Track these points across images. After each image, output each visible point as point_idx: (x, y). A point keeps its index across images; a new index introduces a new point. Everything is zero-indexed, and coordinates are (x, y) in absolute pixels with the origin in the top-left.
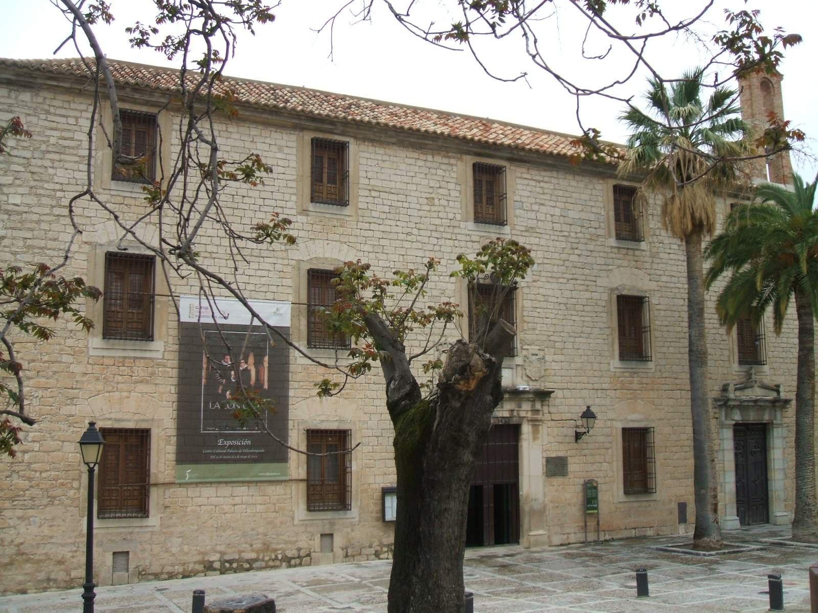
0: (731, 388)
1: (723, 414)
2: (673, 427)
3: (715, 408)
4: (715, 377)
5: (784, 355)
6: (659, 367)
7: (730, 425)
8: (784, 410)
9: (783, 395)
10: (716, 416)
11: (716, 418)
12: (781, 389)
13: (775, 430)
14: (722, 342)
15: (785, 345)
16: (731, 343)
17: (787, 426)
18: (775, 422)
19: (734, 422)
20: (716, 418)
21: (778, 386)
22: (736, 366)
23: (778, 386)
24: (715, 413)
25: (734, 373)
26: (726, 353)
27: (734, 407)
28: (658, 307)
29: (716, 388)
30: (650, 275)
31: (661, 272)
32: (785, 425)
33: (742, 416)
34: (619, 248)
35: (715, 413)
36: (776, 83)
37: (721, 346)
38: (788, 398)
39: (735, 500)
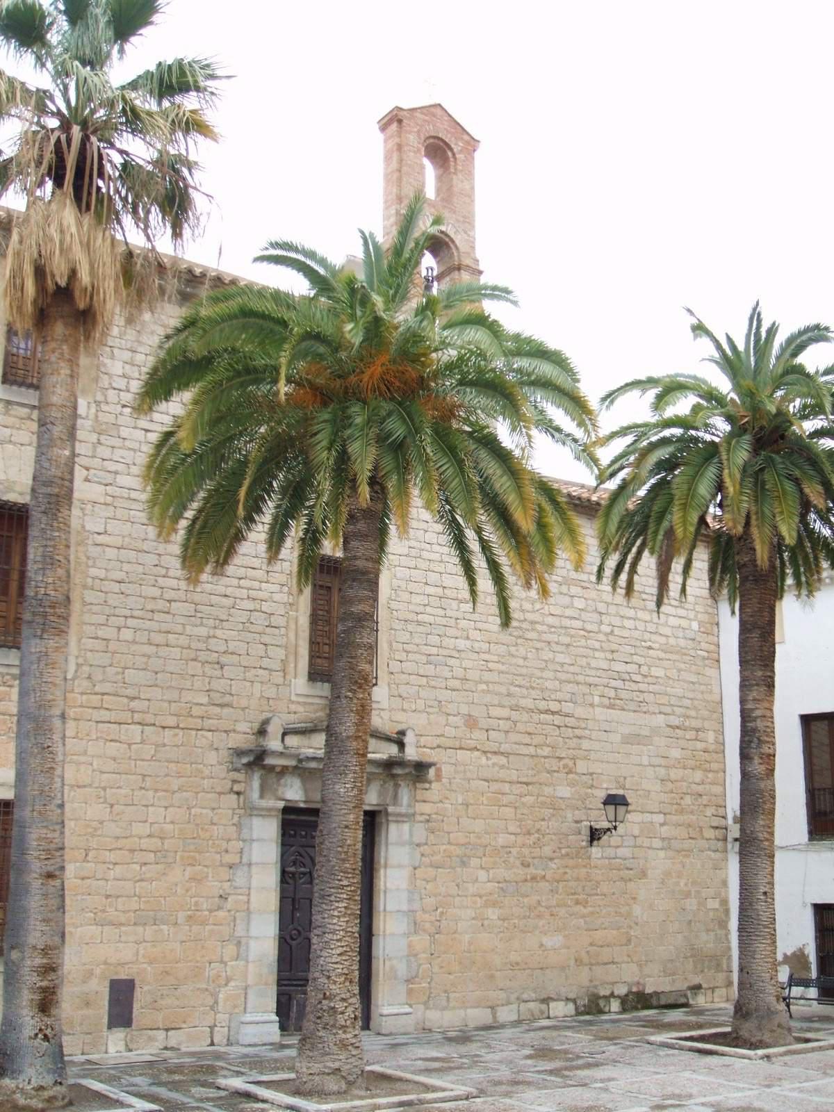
0: (275, 729)
1: (256, 784)
2: (112, 806)
3: (235, 770)
4: (244, 703)
5: (430, 670)
6: (86, 669)
7: (269, 810)
8: (418, 785)
9: (411, 753)
10: (236, 788)
11: (238, 793)
12: (409, 739)
13: (393, 828)
14: (268, 630)
15: (434, 651)
16: (292, 635)
17: (428, 821)
18: (391, 809)
19: (281, 804)
20: (238, 793)
21: (402, 733)
22: (300, 683)
23: (402, 733)
24: (234, 781)
25: (294, 698)
26: (281, 653)
27: (284, 771)
28: (100, 539)
29: (243, 727)
30: (87, 469)
31: (120, 467)
32: (418, 818)
33: (306, 791)
34: (8, 403)
35: (234, 781)
36: (461, 152)
37: (266, 639)
38: (426, 759)
39: (273, 978)
